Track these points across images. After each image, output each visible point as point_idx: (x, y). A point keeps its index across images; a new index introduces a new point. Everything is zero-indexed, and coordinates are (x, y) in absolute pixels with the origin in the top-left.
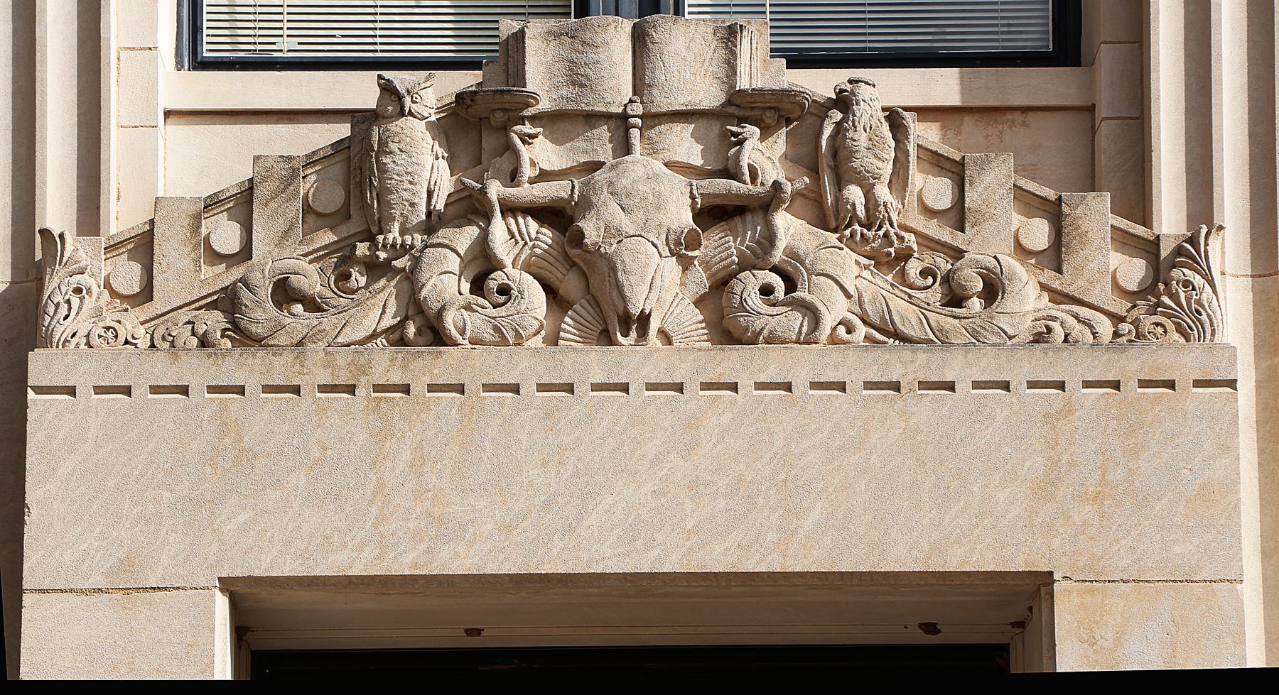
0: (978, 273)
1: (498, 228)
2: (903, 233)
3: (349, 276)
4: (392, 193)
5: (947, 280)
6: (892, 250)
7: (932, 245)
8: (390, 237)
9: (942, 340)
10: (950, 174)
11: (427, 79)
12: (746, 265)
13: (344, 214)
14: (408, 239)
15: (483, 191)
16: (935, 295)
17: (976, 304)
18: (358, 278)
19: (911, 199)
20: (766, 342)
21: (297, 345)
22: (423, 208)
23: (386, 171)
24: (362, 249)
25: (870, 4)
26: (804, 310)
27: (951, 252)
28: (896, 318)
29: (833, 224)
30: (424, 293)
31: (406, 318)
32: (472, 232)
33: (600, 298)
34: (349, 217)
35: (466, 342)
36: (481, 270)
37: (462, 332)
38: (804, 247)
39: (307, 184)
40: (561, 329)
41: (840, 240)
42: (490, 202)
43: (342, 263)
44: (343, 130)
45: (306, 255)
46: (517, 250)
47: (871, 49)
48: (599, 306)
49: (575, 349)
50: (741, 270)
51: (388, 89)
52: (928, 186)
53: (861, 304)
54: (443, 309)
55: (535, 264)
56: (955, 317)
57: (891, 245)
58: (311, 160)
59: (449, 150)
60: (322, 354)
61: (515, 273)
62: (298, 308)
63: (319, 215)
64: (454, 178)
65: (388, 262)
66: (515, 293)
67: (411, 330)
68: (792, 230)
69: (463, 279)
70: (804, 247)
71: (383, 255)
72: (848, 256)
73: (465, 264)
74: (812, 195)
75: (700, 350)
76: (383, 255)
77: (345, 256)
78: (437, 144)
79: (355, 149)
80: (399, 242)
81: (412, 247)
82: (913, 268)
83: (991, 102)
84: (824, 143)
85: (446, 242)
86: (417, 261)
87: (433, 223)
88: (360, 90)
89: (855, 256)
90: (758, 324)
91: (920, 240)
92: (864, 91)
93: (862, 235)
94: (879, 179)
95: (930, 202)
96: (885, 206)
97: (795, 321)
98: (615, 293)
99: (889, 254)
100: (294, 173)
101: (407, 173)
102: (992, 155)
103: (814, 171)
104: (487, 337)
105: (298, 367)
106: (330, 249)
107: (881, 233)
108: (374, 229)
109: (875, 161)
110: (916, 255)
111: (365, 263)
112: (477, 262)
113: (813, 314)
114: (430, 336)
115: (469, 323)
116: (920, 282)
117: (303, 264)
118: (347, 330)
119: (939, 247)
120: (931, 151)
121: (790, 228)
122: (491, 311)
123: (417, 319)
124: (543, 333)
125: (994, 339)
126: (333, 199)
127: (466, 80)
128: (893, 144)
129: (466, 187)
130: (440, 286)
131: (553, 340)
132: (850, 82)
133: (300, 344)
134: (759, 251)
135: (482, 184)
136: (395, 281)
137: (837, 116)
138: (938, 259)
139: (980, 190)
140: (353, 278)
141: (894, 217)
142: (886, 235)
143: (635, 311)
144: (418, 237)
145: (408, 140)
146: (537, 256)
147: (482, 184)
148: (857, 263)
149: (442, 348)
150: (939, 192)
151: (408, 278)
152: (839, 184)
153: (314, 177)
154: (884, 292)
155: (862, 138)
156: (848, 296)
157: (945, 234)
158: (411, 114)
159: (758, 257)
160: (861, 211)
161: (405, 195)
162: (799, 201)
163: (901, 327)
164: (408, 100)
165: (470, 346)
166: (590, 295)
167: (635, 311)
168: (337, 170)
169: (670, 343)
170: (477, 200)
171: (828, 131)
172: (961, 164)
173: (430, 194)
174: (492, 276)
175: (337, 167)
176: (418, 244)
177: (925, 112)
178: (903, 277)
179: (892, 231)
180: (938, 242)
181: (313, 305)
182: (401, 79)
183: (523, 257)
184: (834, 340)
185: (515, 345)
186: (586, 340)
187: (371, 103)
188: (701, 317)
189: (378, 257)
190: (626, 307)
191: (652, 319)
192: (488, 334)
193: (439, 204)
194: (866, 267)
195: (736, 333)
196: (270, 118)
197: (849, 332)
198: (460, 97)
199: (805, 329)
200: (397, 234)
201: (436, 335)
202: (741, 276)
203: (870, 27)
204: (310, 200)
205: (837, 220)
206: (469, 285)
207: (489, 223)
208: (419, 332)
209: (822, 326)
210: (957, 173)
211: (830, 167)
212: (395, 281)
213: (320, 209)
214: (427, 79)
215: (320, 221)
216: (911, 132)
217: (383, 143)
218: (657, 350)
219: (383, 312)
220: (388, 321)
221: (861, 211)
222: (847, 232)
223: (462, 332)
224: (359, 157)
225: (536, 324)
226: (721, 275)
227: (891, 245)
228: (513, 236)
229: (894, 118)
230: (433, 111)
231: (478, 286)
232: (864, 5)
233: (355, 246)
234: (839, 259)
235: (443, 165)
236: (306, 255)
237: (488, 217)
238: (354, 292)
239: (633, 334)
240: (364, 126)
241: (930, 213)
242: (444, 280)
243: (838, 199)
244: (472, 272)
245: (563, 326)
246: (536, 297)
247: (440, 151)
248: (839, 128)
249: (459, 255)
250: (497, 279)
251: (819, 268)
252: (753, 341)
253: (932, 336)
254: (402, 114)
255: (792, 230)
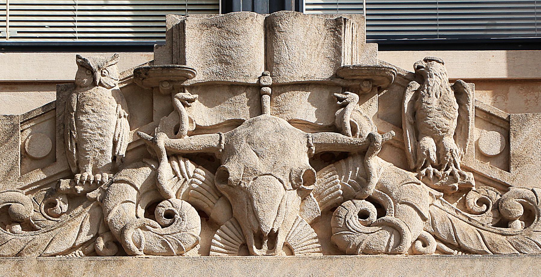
0: (520, 202)
1: (166, 169)
2: (464, 173)
3: (55, 204)
4: (87, 143)
5: (497, 207)
6: (456, 185)
7: (486, 181)
8: (86, 175)
9: (494, 251)
10: (499, 129)
11: (113, 58)
12: (348, 196)
13: (50, 159)
14: (99, 177)
15: (154, 141)
16: (488, 218)
17: (518, 225)
18: (62, 206)
19: (470, 147)
20: (363, 253)
21: (16, 255)
22: (110, 154)
23: (83, 127)
24: (65, 184)
25: (440, 3)
26: (391, 229)
27: (500, 187)
28: (459, 235)
29: (413, 166)
30: (110, 217)
31: (97, 235)
32: (145, 172)
33: (240, 221)
34: (55, 161)
35: (142, 253)
36: (153, 199)
37: (139, 246)
38: (391, 183)
39: (24, 136)
40: (211, 244)
41: (418, 177)
42: (159, 149)
43: (50, 194)
44: (51, 96)
45: (23, 189)
46: (179, 185)
47: (441, 36)
48: (240, 226)
49: (222, 258)
50: (345, 200)
51: (84, 66)
52: (483, 138)
53: (433, 225)
54: (124, 229)
55: (192, 195)
56: (503, 235)
57: (456, 181)
58: (27, 119)
59: (129, 111)
60: (35, 262)
61: (178, 202)
62: (18, 228)
63: (33, 159)
64: (133, 132)
65: (84, 193)
66: (178, 217)
67: (101, 244)
68: (382, 170)
69: (139, 207)
70: (391, 183)
71: (80, 189)
72: (424, 190)
73: (141, 195)
74: (397, 144)
75: (314, 259)
76: (80, 189)
77: (52, 189)
78: (120, 106)
79: (60, 110)
80: (92, 179)
81: (102, 182)
82: (472, 198)
83: (529, 76)
84: (406, 106)
85: (127, 179)
86: (105, 193)
87: (117, 165)
88: (64, 67)
89: (429, 189)
90: (357, 239)
91: (477, 178)
92: (435, 68)
93: (434, 174)
94: (447, 132)
95: (485, 149)
96: (451, 152)
97: (385, 238)
98: (251, 217)
99: (454, 188)
100: (15, 128)
101: (98, 128)
102: (530, 115)
103: (399, 126)
104: (157, 249)
105: (17, 272)
106: (41, 184)
107: (448, 172)
108: (74, 170)
109: (443, 119)
110: (474, 188)
111: (67, 194)
112: (150, 194)
113: (397, 232)
114: (115, 249)
115: (144, 239)
116: (477, 209)
117: (21, 195)
118: (54, 244)
119: (491, 183)
120: (485, 112)
121: (380, 167)
122: (160, 230)
123: (106, 236)
124: (198, 246)
125: (531, 251)
126: (43, 148)
127: (142, 59)
128: (457, 106)
129: (142, 138)
130: (122, 211)
131: (206, 251)
132: (426, 60)
133: (19, 254)
134: (358, 186)
135: (154, 136)
136: (89, 208)
137: (416, 85)
138: (490, 192)
139: (521, 140)
140: (58, 206)
141: (458, 161)
142: (452, 174)
143: (266, 230)
144: (106, 175)
145: (99, 103)
146: (194, 189)
147: (154, 136)
148: (431, 194)
149: (124, 258)
150: (491, 141)
151: (99, 206)
152: (418, 136)
153: (29, 131)
154: (450, 216)
155: (434, 102)
156: (424, 219)
157: (496, 173)
158: (101, 84)
159: (358, 189)
160: (433, 156)
161: (97, 144)
162: (387, 149)
163: (463, 242)
164: (98, 74)
165: (144, 256)
166: (233, 218)
167: (266, 230)
168: (46, 126)
169: (292, 254)
170: (150, 148)
171: (409, 97)
172: (508, 121)
173: (115, 143)
174: (161, 204)
175: (47, 123)
176: (106, 180)
177: (481, 83)
178: (464, 205)
179: (456, 171)
180: (491, 179)
181: (29, 226)
182: (93, 58)
183: (184, 190)
184: (413, 251)
185: (178, 255)
186: (230, 252)
187: (72, 77)
188: (315, 235)
189: (76, 190)
190: (259, 227)
191: (279, 236)
192: (157, 247)
193: (122, 151)
194: (438, 198)
195: (341, 246)
196: (19, 87)
197: (424, 245)
198: (137, 71)
199: (392, 244)
200: (90, 173)
201: (119, 248)
202: (345, 204)
203: (440, 20)
204: (26, 148)
205: (416, 162)
206: (143, 211)
207: (159, 165)
208: (106, 246)
209: (405, 241)
210: (505, 128)
211: (410, 123)
212: (89, 208)
213: (34, 155)
214: (113, 58)
215: (34, 164)
216: (471, 98)
217: (80, 105)
218: (283, 259)
219: (81, 231)
220: (84, 238)
221: (433, 156)
222: (423, 172)
223: (139, 246)
224: (62, 116)
225: (193, 240)
226: (330, 203)
227: (456, 181)
228: (176, 175)
229: (458, 87)
230: (117, 82)
231: (150, 212)
232: (435, 3)
233: (60, 182)
234: (417, 192)
235: (125, 122)
236: (23, 189)
237: (158, 161)
238: (59, 216)
239: (265, 247)
240: (66, 94)
241: (484, 157)
242: (125, 207)
243: (417, 147)
244: (146, 201)
245: (214, 241)
246: (193, 220)
247: (123, 112)
248: (417, 94)
249: (136, 189)
250: (164, 206)
251: (402, 198)
252: (354, 252)
253: (486, 249)
254: (94, 84)
255: (382, 170)
